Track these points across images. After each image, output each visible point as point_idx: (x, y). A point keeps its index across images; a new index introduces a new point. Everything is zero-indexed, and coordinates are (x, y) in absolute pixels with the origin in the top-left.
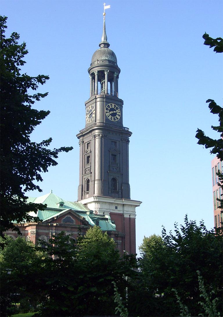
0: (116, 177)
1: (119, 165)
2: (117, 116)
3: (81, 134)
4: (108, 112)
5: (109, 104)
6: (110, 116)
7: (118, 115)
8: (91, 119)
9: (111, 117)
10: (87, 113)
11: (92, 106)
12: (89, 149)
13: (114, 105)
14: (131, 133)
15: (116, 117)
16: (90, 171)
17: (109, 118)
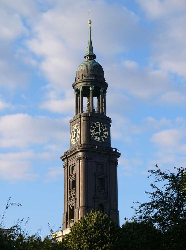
0: (103, 203)
1: (106, 190)
2: (104, 136)
3: (65, 157)
4: (94, 133)
5: (95, 124)
6: (96, 136)
7: (105, 134)
8: (76, 140)
9: (98, 138)
10: (72, 133)
11: (76, 126)
12: (74, 173)
13: (101, 124)
14: (120, 154)
15: (103, 137)
16: (75, 197)
17: (95, 139)
